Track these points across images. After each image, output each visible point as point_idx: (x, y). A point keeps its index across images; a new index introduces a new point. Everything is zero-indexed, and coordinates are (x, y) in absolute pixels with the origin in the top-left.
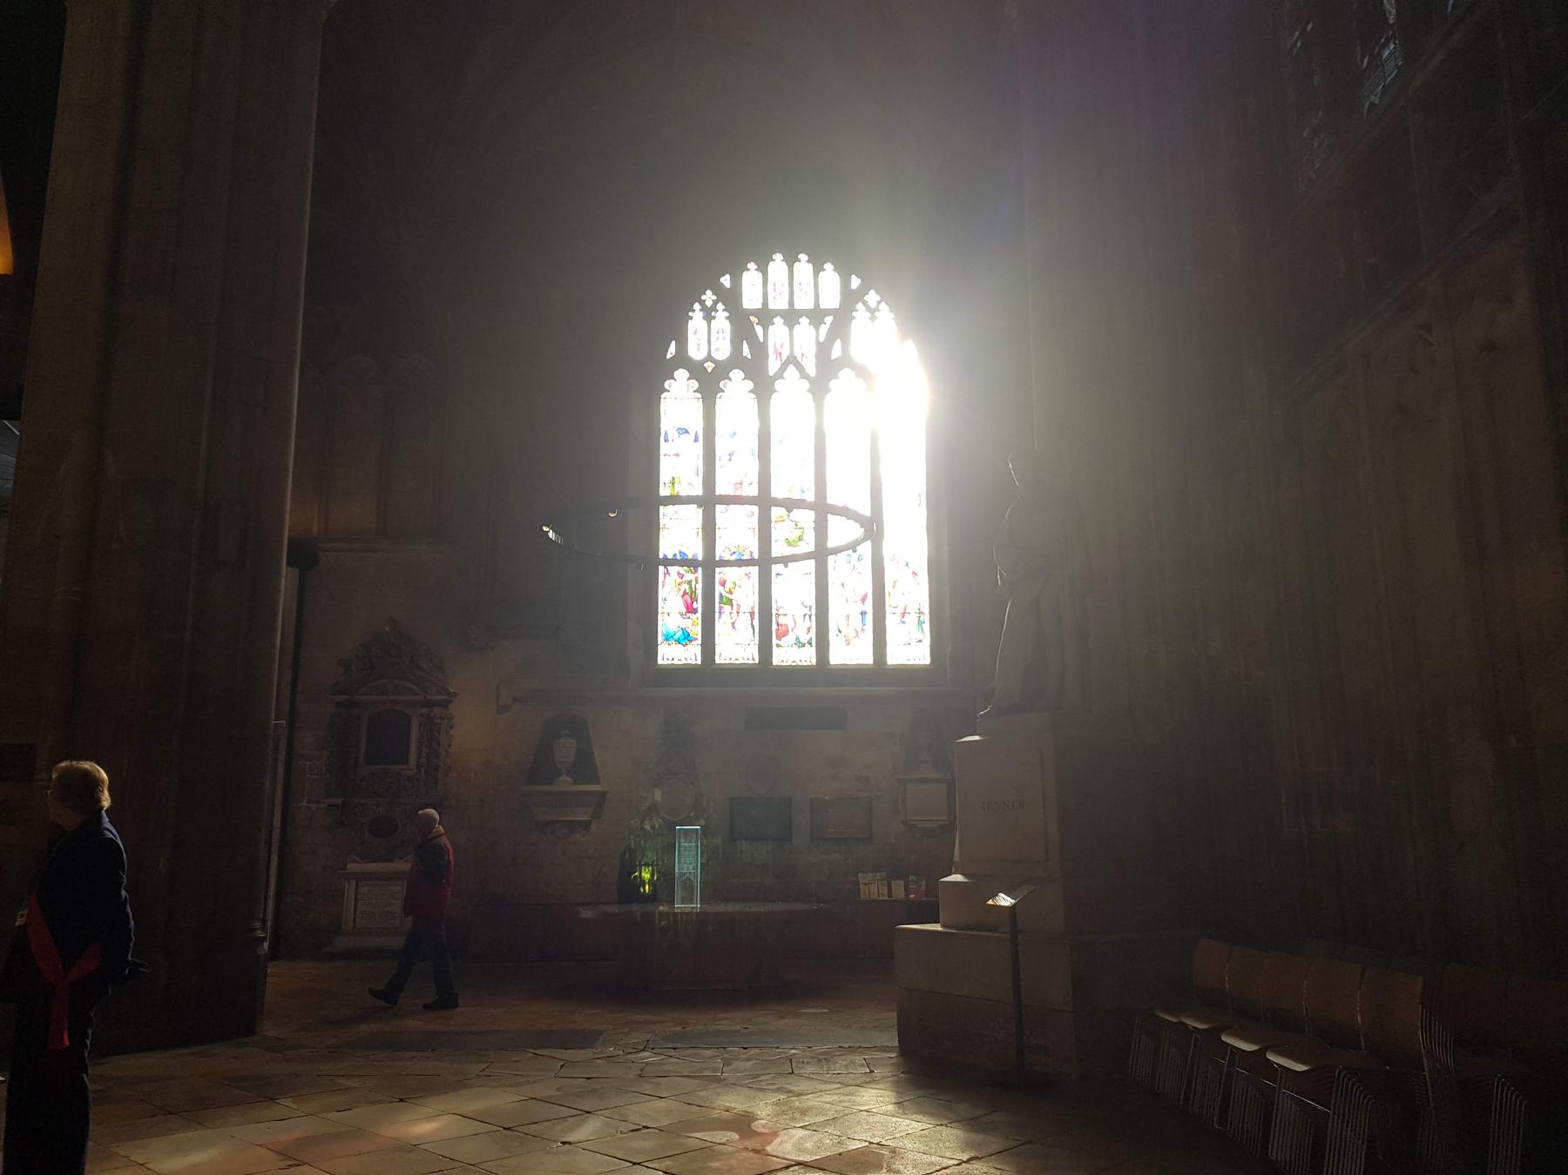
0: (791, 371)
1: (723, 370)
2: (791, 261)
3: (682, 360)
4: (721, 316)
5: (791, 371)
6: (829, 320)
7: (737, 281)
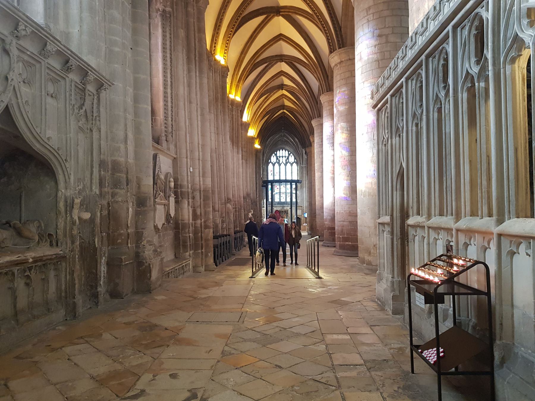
0: (282, 163)
1: (275, 163)
2: (282, 150)
3: (271, 162)
4: (275, 156)
5: (282, 163)
6: (286, 157)
7: (277, 153)
